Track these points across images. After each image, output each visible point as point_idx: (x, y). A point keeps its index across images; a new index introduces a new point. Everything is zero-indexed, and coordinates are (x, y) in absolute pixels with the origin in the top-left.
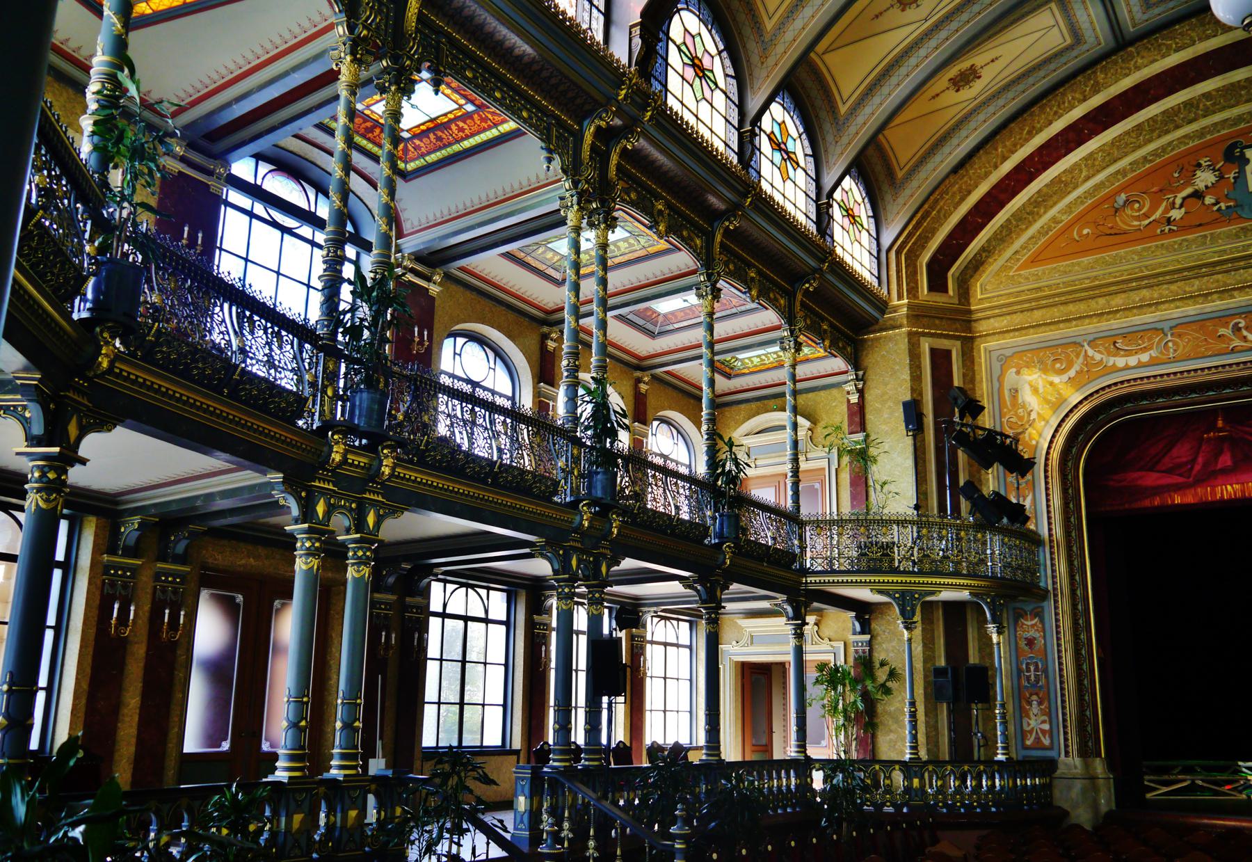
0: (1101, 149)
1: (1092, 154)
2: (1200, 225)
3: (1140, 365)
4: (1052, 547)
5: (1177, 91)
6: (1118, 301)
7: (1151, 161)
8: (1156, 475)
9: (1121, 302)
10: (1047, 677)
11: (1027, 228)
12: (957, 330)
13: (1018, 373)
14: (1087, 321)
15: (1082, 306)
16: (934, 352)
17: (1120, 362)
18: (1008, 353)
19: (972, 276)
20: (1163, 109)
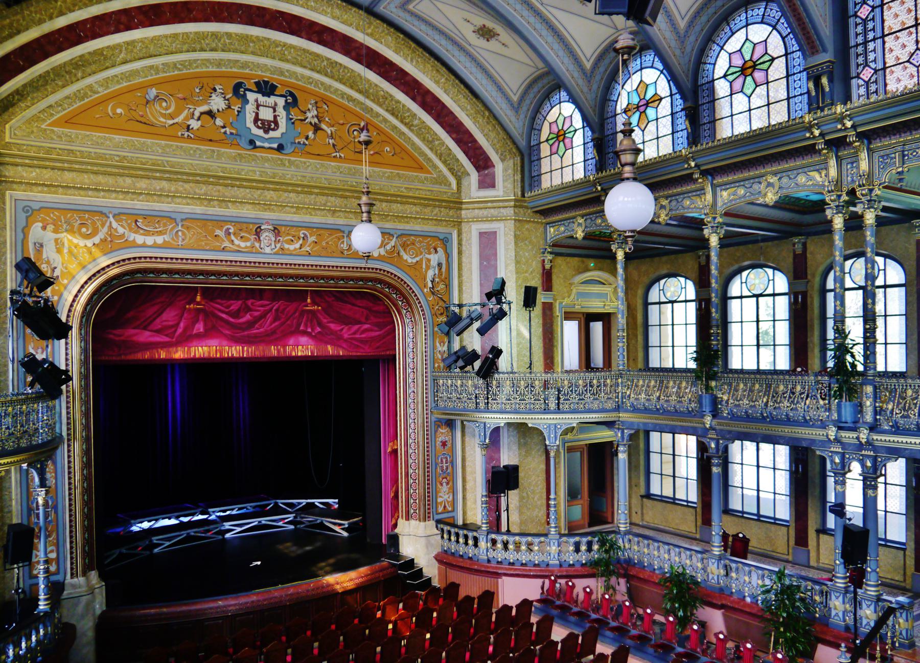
0: (142, 41)
1: (133, 42)
2: (211, 140)
3: (155, 246)
4: (68, 397)
5: (212, 21)
6: (142, 184)
7: (179, 70)
8: (147, 333)
9: (144, 186)
10: (56, 512)
11: (64, 86)
13: (44, 228)
14: (114, 195)
15: (111, 180)
17: (140, 239)
18: (36, 206)
20: (197, 30)
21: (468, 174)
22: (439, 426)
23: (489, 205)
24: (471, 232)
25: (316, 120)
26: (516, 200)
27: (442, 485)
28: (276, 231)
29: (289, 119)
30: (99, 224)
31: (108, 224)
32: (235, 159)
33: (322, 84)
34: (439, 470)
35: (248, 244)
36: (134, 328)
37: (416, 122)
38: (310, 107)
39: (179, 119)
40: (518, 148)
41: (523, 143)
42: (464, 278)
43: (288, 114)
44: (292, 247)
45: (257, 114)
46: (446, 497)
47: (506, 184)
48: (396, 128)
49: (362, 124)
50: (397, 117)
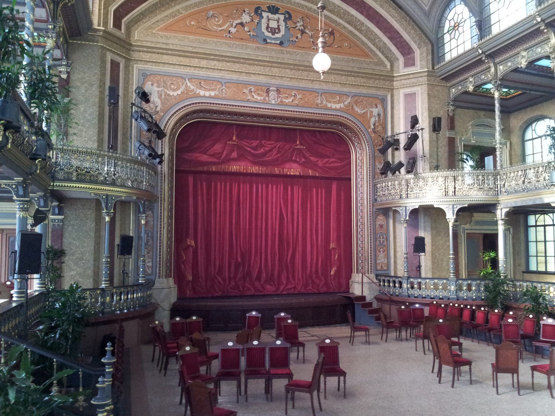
3: (210, 97)
6: (204, 63)
11: (164, 11)
12: (123, 53)
13: (152, 85)
16: (112, 62)
19: (133, 26)
21: (398, 59)
22: (378, 215)
23: (411, 76)
24: (399, 94)
25: (302, 27)
26: (428, 71)
27: (380, 252)
28: (278, 91)
29: (286, 27)
30: (180, 84)
31: (185, 84)
32: (255, 49)
33: (306, 7)
34: (378, 242)
35: (262, 98)
36: (199, 153)
37: (364, 28)
38: (299, 20)
39: (225, 27)
40: (429, 40)
41: (433, 37)
42: (395, 124)
43: (286, 24)
44: (287, 101)
45: (268, 24)
46: (383, 260)
47: (422, 63)
48: (351, 32)
49: (330, 30)
50: (352, 25)
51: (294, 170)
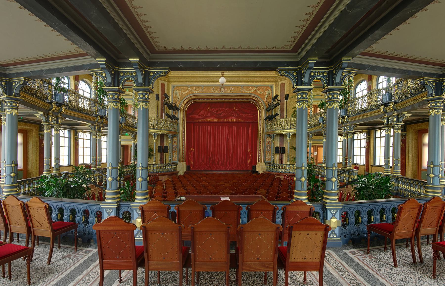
3: (198, 93)
15: (189, 79)
28: (224, 88)
51: (233, 120)
